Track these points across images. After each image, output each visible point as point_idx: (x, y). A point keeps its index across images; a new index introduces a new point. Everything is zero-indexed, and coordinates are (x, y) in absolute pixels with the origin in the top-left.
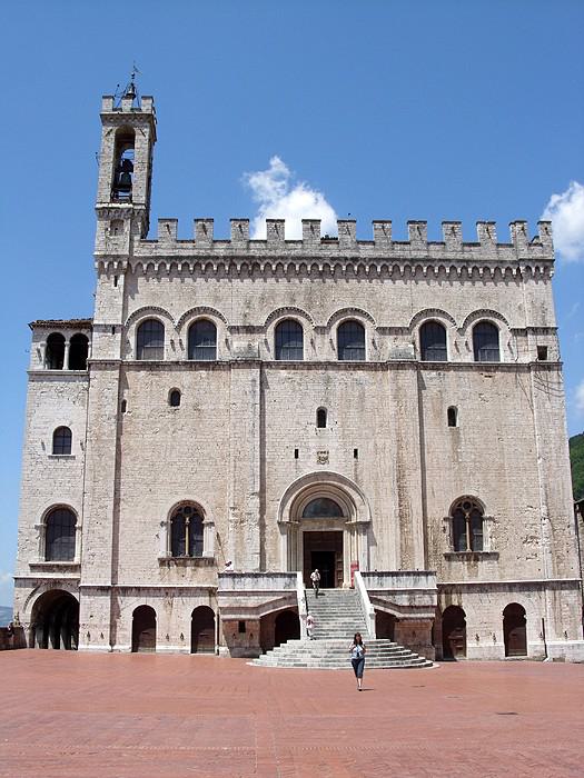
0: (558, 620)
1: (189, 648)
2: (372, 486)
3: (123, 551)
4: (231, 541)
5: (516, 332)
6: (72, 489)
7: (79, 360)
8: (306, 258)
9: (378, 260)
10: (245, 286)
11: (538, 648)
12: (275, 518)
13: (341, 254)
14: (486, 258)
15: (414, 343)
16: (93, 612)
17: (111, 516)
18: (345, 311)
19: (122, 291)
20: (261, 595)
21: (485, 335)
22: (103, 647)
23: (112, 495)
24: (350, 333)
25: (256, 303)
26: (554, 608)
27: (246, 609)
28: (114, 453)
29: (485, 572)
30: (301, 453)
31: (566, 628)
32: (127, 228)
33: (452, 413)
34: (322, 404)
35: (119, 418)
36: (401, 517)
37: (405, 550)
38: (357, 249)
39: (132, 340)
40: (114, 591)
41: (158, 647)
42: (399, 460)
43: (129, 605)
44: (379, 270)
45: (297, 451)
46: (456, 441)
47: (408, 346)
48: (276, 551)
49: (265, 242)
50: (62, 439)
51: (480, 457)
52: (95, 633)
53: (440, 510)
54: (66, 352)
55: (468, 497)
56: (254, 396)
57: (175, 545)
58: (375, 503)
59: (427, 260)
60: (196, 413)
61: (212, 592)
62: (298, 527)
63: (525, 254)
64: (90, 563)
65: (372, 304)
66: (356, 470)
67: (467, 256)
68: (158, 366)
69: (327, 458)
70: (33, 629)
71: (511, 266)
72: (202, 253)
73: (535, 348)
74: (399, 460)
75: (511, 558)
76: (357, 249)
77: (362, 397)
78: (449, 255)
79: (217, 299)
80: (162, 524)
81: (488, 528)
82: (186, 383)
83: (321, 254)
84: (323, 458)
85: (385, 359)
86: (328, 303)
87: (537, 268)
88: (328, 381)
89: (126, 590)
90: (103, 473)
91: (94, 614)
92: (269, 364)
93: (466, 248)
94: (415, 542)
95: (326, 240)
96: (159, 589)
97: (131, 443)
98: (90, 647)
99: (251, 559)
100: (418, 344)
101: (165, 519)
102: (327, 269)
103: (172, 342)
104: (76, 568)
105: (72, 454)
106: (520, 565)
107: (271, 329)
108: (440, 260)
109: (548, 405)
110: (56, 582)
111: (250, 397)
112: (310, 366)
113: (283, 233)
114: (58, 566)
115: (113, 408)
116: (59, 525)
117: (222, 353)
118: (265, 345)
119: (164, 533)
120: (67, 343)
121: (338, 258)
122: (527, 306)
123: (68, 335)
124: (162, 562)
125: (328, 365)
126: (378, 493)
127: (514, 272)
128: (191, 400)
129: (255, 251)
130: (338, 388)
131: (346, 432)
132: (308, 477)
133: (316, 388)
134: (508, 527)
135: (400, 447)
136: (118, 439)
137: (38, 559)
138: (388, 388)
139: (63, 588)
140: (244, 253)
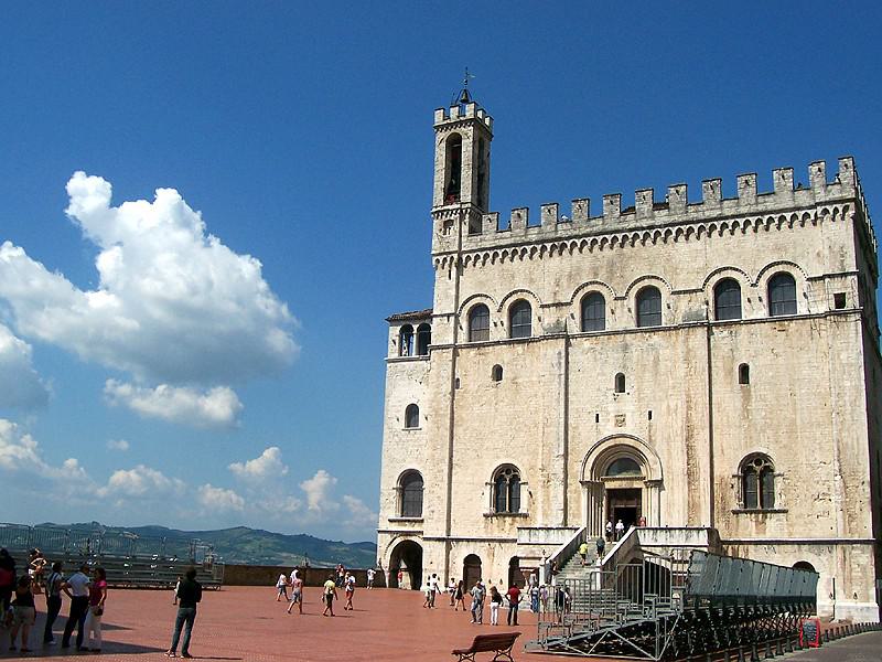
0: (848, 580)
2: (664, 447)
9: (673, 225)
10: (556, 264)
11: (826, 609)
13: (638, 225)
14: (781, 207)
15: (707, 304)
16: (432, 557)
21: (780, 285)
23: (447, 460)
24: (648, 297)
25: (564, 282)
29: (774, 528)
30: (601, 418)
32: (456, 226)
33: (744, 369)
36: (689, 475)
37: (693, 507)
38: (653, 217)
39: (464, 324)
40: (448, 541)
42: (688, 419)
43: (461, 553)
46: (747, 397)
47: (703, 304)
48: (578, 510)
50: (412, 412)
51: (771, 413)
53: (728, 467)
55: (758, 454)
56: (559, 368)
57: (497, 502)
58: (665, 459)
63: (822, 197)
67: (761, 208)
68: (484, 345)
70: (395, 571)
71: (809, 211)
72: (518, 240)
74: (688, 419)
75: (800, 516)
76: (653, 217)
77: (656, 362)
78: (744, 210)
79: (532, 281)
81: (779, 485)
83: (620, 227)
86: (627, 274)
87: (836, 210)
88: (626, 348)
89: (458, 540)
90: (440, 442)
92: (574, 337)
93: (760, 199)
94: (702, 499)
97: (464, 415)
99: (558, 510)
100: (711, 303)
103: (495, 325)
104: (422, 521)
106: (811, 523)
108: (733, 217)
109: (843, 356)
112: (608, 334)
114: (409, 521)
116: (411, 482)
117: (537, 330)
118: (572, 319)
119: (488, 492)
120: (415, 332)
122: (826, 252)
123: (415, 327)
127: (813, 218)
130: (634, 354)
135: (689, 408)
136: (452, 412)
137: (394, 513)
138: (680, 349)
139: (413, 539)
140: (553, 235)
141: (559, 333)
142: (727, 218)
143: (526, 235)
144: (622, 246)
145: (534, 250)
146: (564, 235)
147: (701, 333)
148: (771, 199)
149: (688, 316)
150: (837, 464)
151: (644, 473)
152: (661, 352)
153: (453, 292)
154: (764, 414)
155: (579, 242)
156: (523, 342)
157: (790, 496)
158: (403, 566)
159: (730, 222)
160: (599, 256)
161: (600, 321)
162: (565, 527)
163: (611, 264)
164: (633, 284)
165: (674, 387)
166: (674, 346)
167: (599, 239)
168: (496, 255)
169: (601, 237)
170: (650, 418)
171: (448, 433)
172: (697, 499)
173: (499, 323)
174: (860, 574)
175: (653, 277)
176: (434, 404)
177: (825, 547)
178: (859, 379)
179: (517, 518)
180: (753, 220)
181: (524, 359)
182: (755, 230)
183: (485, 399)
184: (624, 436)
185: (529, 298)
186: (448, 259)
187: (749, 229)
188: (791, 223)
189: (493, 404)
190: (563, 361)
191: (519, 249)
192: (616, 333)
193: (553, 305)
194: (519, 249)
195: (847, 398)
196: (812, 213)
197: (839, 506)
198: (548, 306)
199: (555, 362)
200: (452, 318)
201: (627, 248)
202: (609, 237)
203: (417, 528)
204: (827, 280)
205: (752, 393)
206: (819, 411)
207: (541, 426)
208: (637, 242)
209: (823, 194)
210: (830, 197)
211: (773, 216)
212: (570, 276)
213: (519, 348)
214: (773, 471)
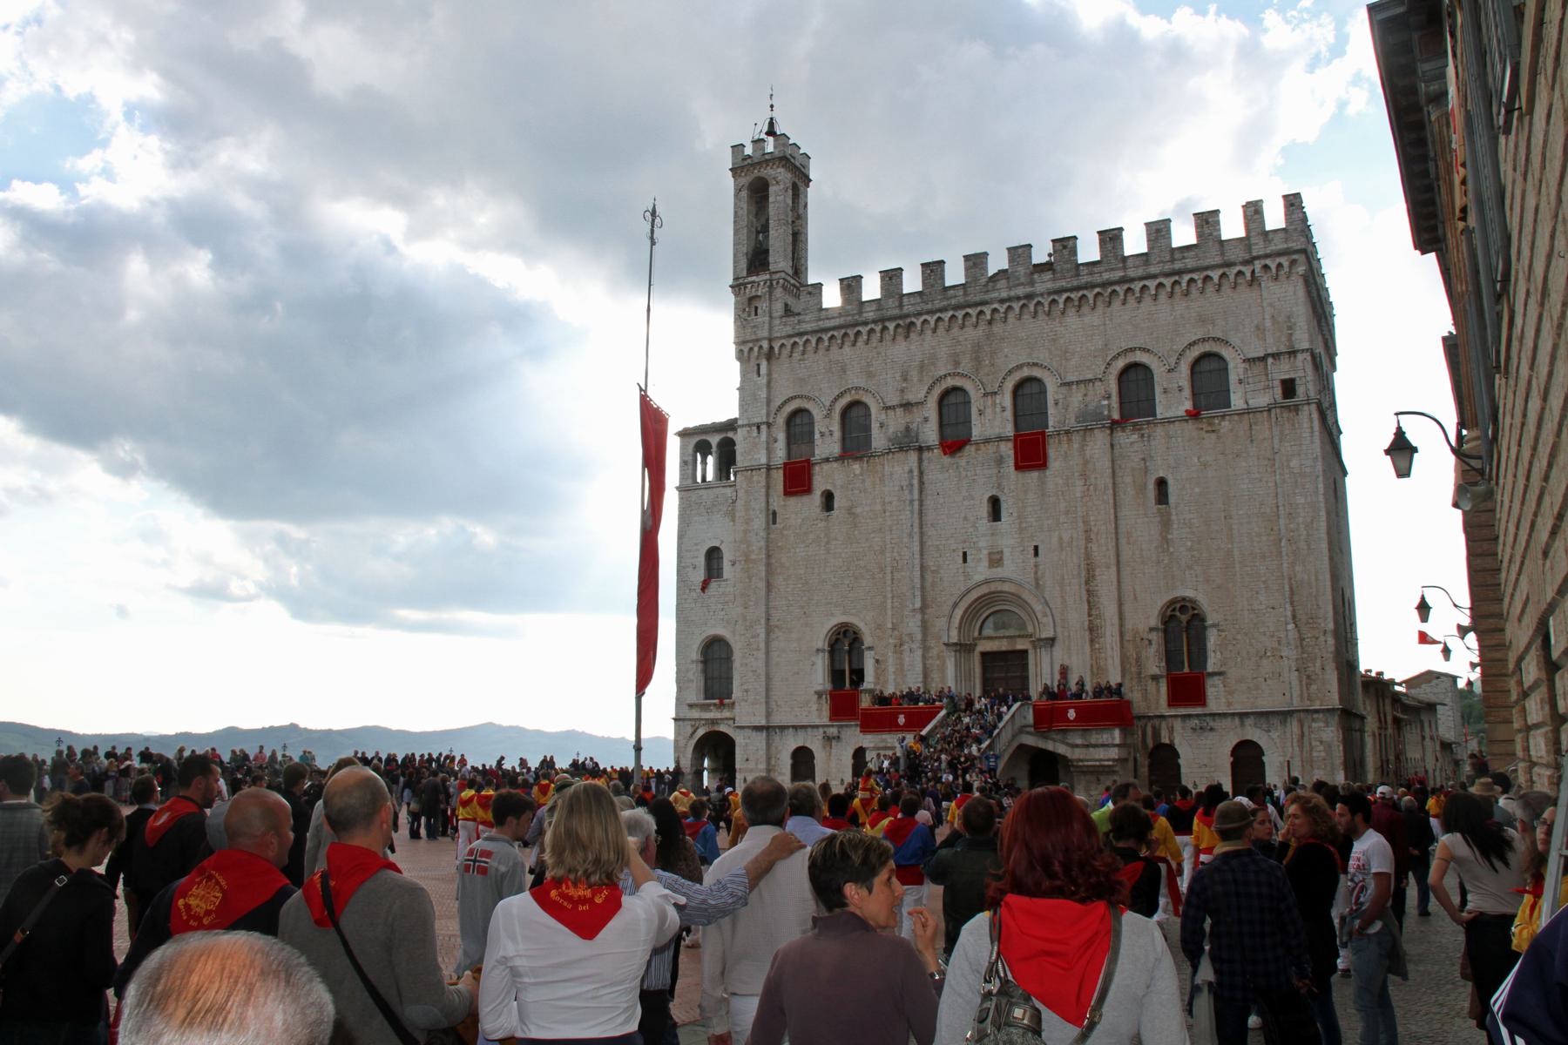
4: (891, 669)
9: (1060, 291)
10: (901, 351)
13: (1012, 294)
14: (1206, 263)
17: (762, 645)
18: (1019, 367)
19: (765, 381)
23: (763, 622)
25: (914, 374)
26: (1301, 746)
32: (763, 305)
33: (1162, 484)
34: (994, 493)
35: (768, 527)
36: (1091, 630)
39: (781, 437)
42: (1088, 555)
45: (965, 554)
46: (1166, 524)
50: (713, 555)
53: (1146, 616)
55: (1184, 599)
56: (911, 492)
67: (1178, 266)
71: (1243, 269)
73: (1277, 383)
74: (1088, 555)
76: (1032, 283)
78: (1153, 270)
79: (870, 375)
82: (839, 483)
83: (986, 297)
84: (996, 560)
85: (1071, 422)
87: (1280, 266)
89: (783, 728)
92: (929, 448)
94: (1110, 661)
96: (817, 727)
103: (822, 435)
106: (1257, 688)
109: (1294, 463)
110: (714, 722)
115: (759, 522)
117: (878, 440)
120: (714, 448)
121: (1009, 299)
122: (1268, 324)
123: (714, 440)
126: (1064, 601)
127: (1248, 275)
129: (907, 309)
132: (979, 585)
135: (1088, 540)
139: (723, 728)
140: (896, 312)
141: (907, 443)
142: (1132, 280)
143: (860, 313)
144: (990, 322)
145: (871, 331)
146: (912, 309)
147: (1100, 439)
149: (1082, 416)
150: (1288, 606)
151: (1030, 629)
153: (763, 394)
155: (932, 319)
156: (860, 459)
158: (706, 764)
159: (1137, 286)
163: (977, 348)
166: (1066, 456)
167: (960, 314)
168: (819, 340)
170: (1036, 554)
171: (762, 585)
175: (1035, 364)
177: (1275, 721)
178: (1316, 492)
180: (1168, 282)
182: (1171, 295)
183: (811, 536)
184: (1002, 580)
185: (866, 399)
187: (1163, 296)
188: (1220, 285)
190: (916, 482)
191: (851, 332)
192: (987, 441)
193: (901, 405)
194: (851, 332)
196: (1247, 270)
197: (1293, 665)
198: (892, 408)
199: (905, 483)
200: (764, 428)
201: (998, 328)
202: (973, 312)
203: (726, 714)
204: (1270, 360)
205: (1174, 517)
207: (889, 569)
208: (1011, 316)
209: (1261, 244)
210: (1272, 248)
211: (1195, 276)
212: (922, 367)
213: (856, 467)
214: (1203, 620)
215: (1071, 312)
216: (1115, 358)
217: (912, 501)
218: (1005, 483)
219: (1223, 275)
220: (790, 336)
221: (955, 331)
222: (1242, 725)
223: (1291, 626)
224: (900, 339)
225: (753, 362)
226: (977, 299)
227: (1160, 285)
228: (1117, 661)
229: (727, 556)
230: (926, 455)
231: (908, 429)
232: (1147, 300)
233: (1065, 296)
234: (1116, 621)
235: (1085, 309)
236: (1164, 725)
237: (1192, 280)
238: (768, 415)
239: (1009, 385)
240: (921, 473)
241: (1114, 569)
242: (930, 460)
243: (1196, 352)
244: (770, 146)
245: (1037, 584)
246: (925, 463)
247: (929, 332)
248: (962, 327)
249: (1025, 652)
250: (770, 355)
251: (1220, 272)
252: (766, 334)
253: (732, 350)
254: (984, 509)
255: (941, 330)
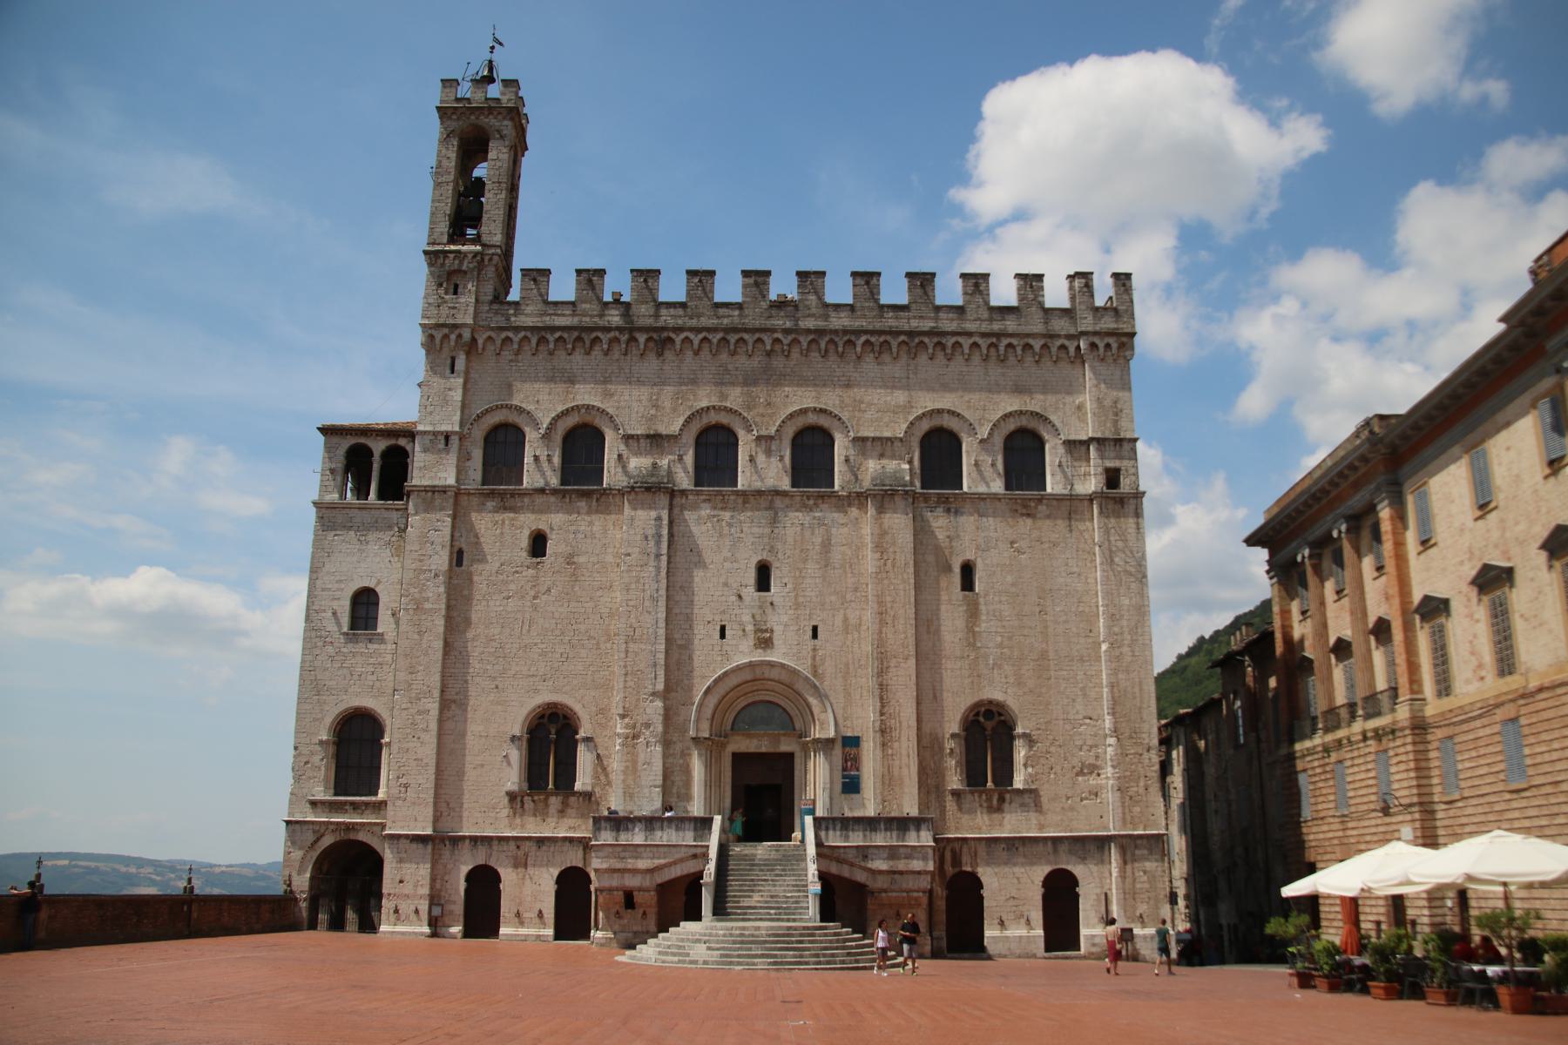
1: (550, 932)
3: (451, 782)
5: (1071, 445)
6: (378, 684)
7: (395, 483)
8: (746, 330)
9: (858, 332)
11: (1097, 940)
12: (687, 731)
15: (910, 462)
17: (434, 726)
18: (803, 411)
20: (653, 855)
22: (418, 929)
23: (436, 693)
27: (635, 871)
28: (441, 629)
31: (1142, 908)
34: (765, 556)
37: (888, 781)
41: (504, 930)
42: (880, 643)
44: (859, 349)
45: (723, 629)
49: (683, 305)
51: (1010, 638)
52: (406, 907)
54: (376, 466)
55: (990, 702)
56: (658, 543)
59: (931, 333)
60: (570, 569)
61: (584, 844)
62: (723, 746)
64: (402, 803)
65: (847, 401)
66: (814, 658)
67: (996, 327)
69: (770, 638)
70: (314, 901)
71: (1067, 343)
72: (587, 321)
75: (1055, 798)
76: (826, 317)
77: (827, 546)
78: (970, 326)
80: (513, 739)
81: (1020, 753)
87: (1108, 346)
91: (407, 878)
92: (683, 492)
94: (905, 771)
95: (782, 304)
96: (507, 839)
98: (399, 928)
101: (517, 731)
102: (777, 347)
103: (536, 458)
104: (383, 804)
105: (379, 630)
106: (1072, 809)
107: (689, 439)
110: (350, 827)
111: (652, 543)
112: (744, 494)
113: (712, 291)
114: (353, 804)
115: (441, 560)
117: (612, 476)
119: (516, 755)
123: (378, 447)
124: (512, 796)
125: (777, 493)
126: (848, 694)
127: (1072, 350)
128: (562, 548)
129: (667, 318)
131: (801, 599)
132: (738, 668)
133: (755, 530)
134: (1052, 749)
135: (883, 623)
138: (867, 529)
139: (362, 836)
140: (649, 322)
143: (601, 316)
144: (769, 354)
146: (671, 322)
148: (1012, 317)
149: (879, 480)
151: (798, 726)
152: (834, 531)
153: (457, 395)
154: (999, 639)
155: (696, 339)
156: (586, 495)
157: (1039, 768)
159: (951, 341)
160: (730, 367)
161: (728, 473)
162: (669, 816)
164: (791, 416)
165: (856, 590)
167: (733, 338)
168: (542, 340)
169: (737, 337)
170: (815, 635)
171: (439, 644)
172: (896, 773)
173: (543, 458)
174: (1147, 886)
175: (822, 411)
176: (412, 590)
179: (572, 799)
180: (983, 343)
181: (591, 523)
183: (512, 587)
184: (771, 665)
186: (453, 337)
187: (976, 359)
188: (1041, 356)
189: (529, 598)
190: (665, 532)
192: (759, 493)
193: (648, 436)
195: (1125, 623)
199: (651, 532)
201: (778, 362)
205: (983, 608)
206: (1082, 640)
208: (795, 354)
211: (1014, 341)
215: (869, 358)
216: (919, 418)
217: (658, 556)
218: (779, 546)
219: (1045, 346)
220: (502, 329)
221: (724, 356)
222: (1055, 851)
223: (1112, 741)
224: (652, 356)
225: (446, 353)
226: (757, 324)
227: (975, 345)
228: (914, 769)
229: (387, 601)
230: (677, 501)
231: (655, 465)
232: (959, 359)
233: (863, 338)
234: (914, 723)
235: (886, 357)
236: (965, 850)
237: (1010, 345)
238: (462, 425)
239: (790, 431)
240: (671, 522)
241: (912, 662)
242: (683, 508)
243: (1011, 426)
244: (494, 91)
245: (815, 673)
246: (676, 511)
247: (689, 353)
248: (733, 353)
249: (791, 756)
250: (471, 348)
251: (1042, 342)
252: (470, 321)
253: (418, 336)
254: (751, 577)
255: (705, 353)
